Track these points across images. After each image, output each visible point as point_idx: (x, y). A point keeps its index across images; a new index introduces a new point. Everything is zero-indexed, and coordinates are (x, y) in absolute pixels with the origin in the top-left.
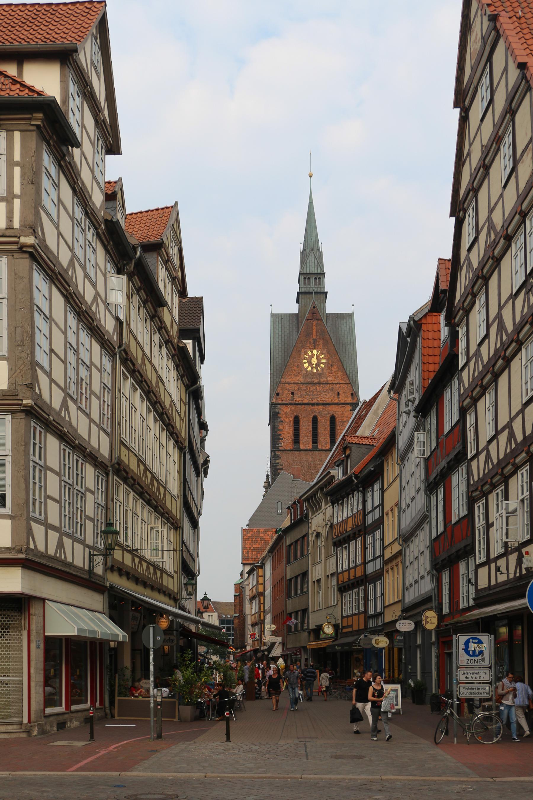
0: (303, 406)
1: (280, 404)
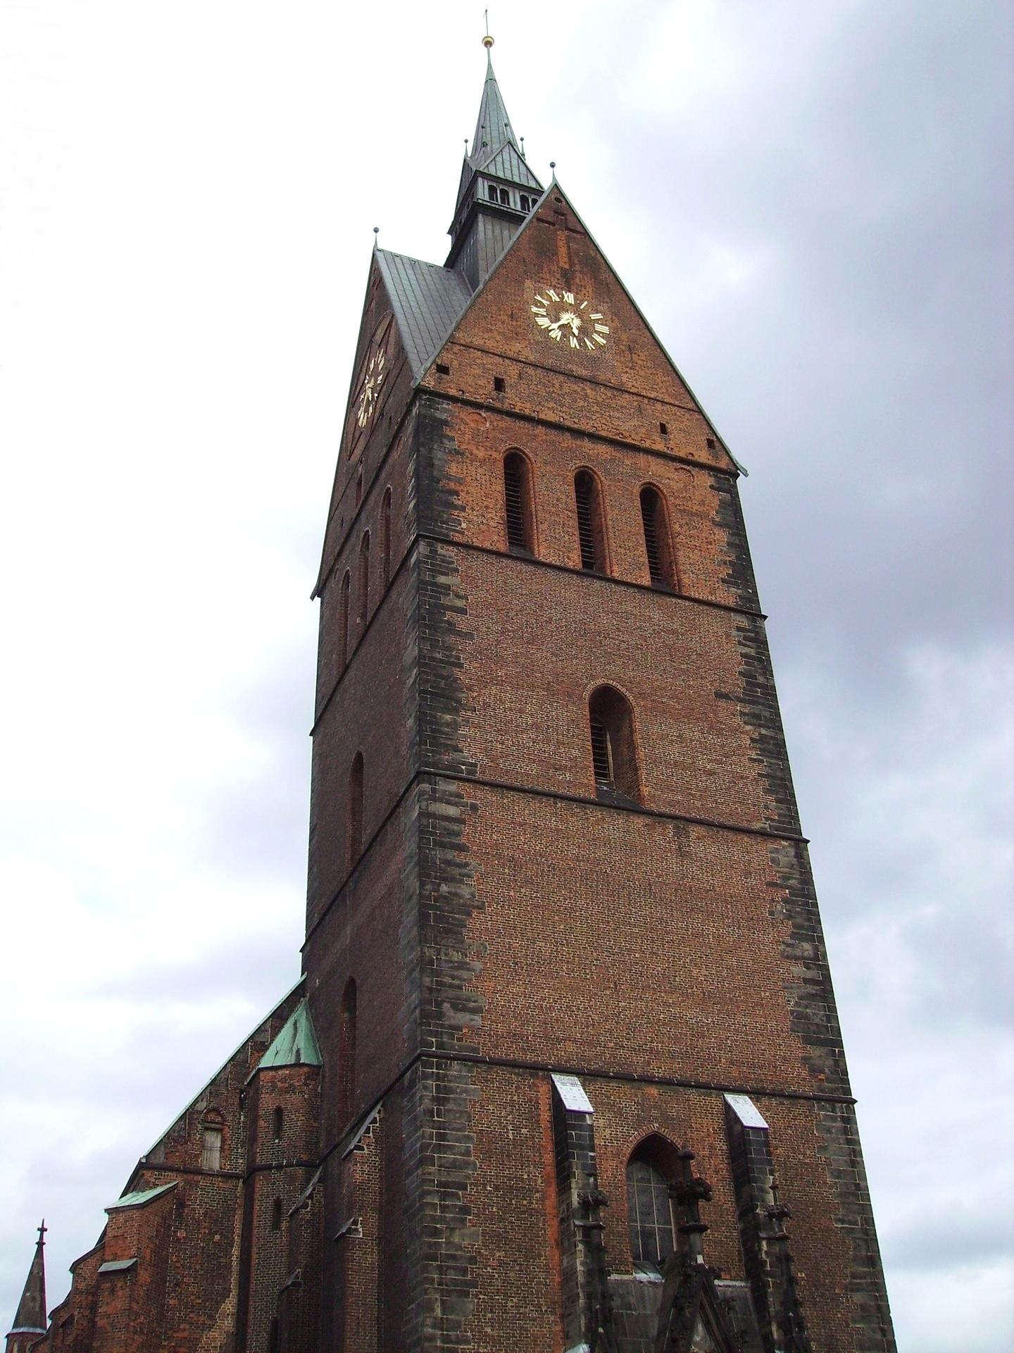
0: (540, 430)
1: (454, 400)
